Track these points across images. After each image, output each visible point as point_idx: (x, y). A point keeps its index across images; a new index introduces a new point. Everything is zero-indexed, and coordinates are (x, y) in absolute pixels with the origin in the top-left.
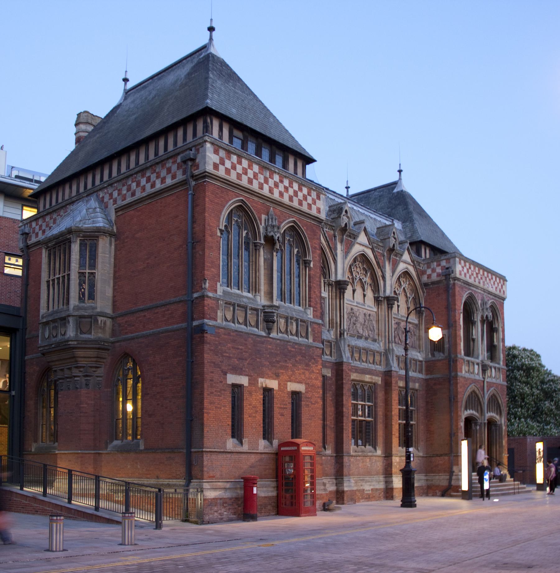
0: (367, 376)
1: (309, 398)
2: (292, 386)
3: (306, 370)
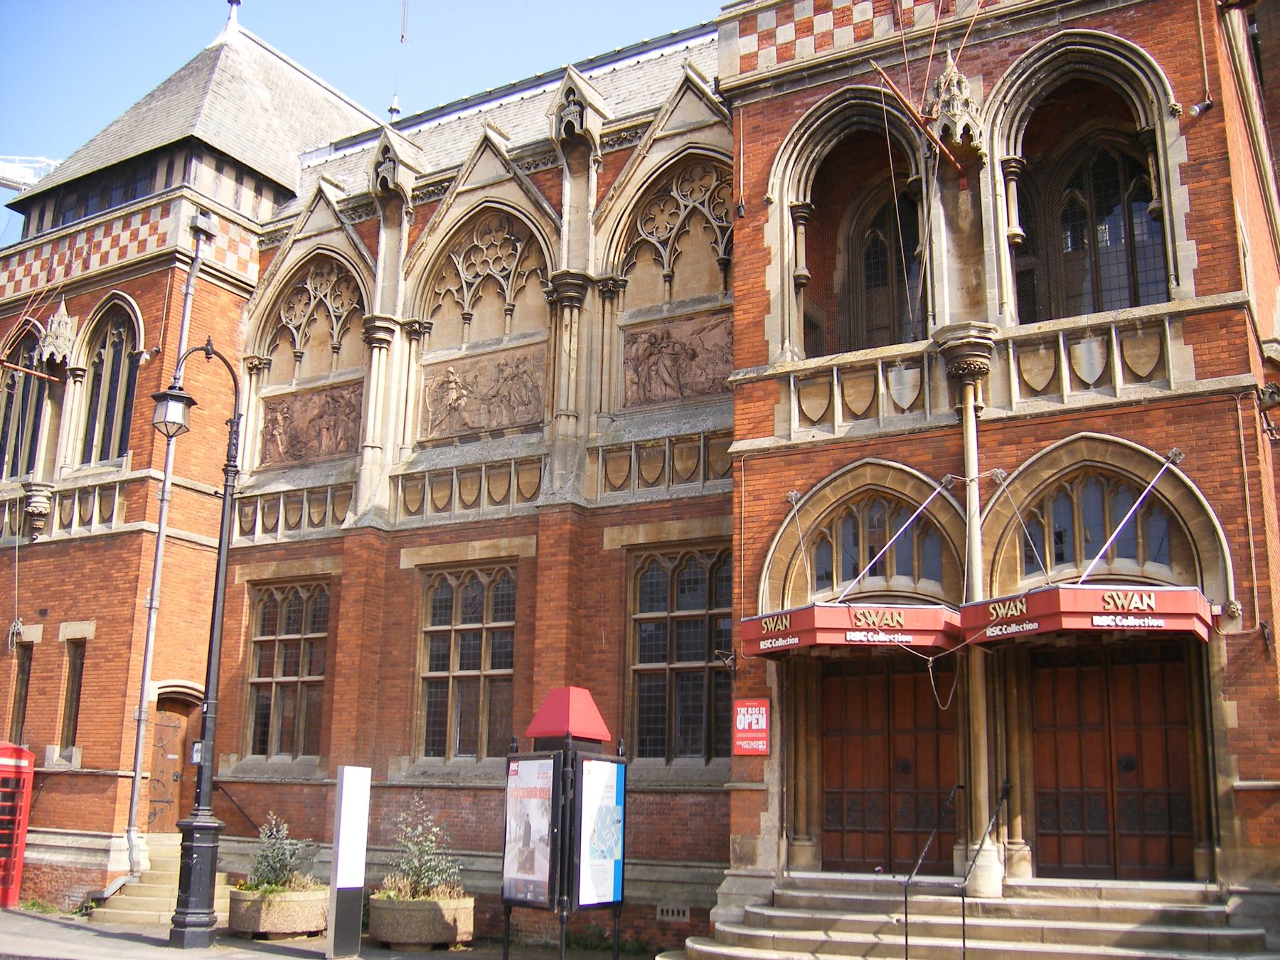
0: (477, 544)
1: (100, 649)
2: (70, 630)
3: (102, 588)
